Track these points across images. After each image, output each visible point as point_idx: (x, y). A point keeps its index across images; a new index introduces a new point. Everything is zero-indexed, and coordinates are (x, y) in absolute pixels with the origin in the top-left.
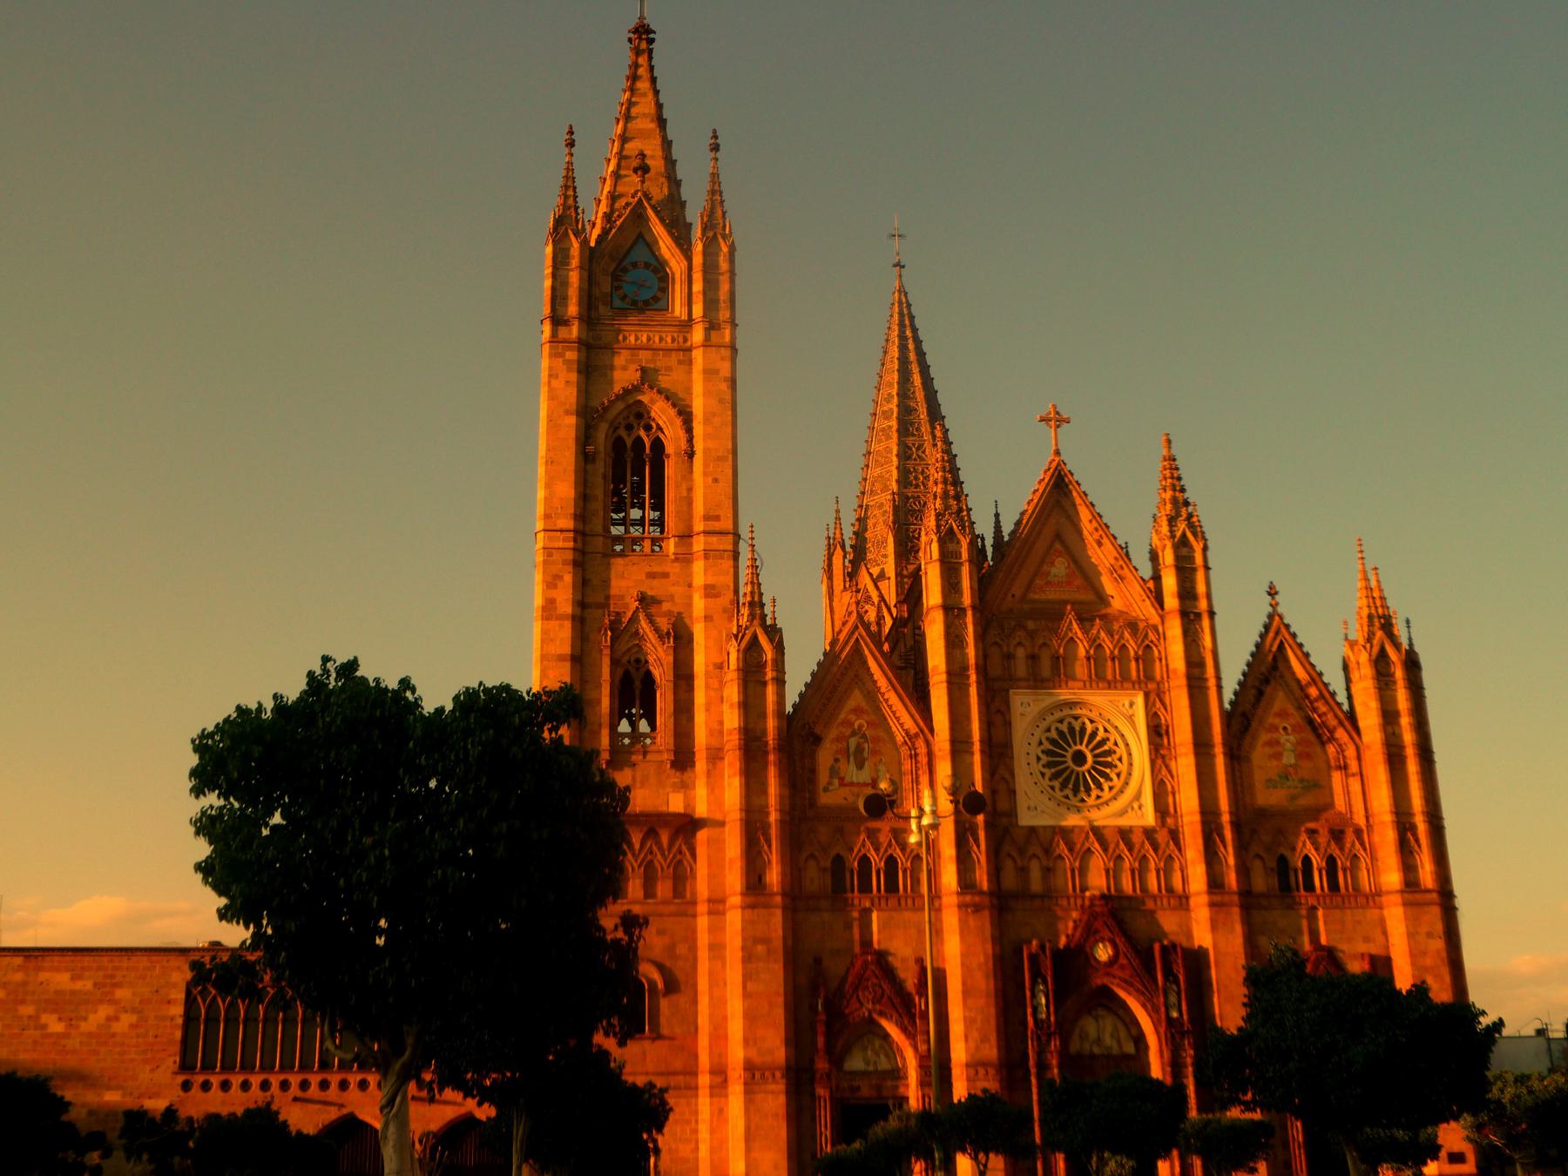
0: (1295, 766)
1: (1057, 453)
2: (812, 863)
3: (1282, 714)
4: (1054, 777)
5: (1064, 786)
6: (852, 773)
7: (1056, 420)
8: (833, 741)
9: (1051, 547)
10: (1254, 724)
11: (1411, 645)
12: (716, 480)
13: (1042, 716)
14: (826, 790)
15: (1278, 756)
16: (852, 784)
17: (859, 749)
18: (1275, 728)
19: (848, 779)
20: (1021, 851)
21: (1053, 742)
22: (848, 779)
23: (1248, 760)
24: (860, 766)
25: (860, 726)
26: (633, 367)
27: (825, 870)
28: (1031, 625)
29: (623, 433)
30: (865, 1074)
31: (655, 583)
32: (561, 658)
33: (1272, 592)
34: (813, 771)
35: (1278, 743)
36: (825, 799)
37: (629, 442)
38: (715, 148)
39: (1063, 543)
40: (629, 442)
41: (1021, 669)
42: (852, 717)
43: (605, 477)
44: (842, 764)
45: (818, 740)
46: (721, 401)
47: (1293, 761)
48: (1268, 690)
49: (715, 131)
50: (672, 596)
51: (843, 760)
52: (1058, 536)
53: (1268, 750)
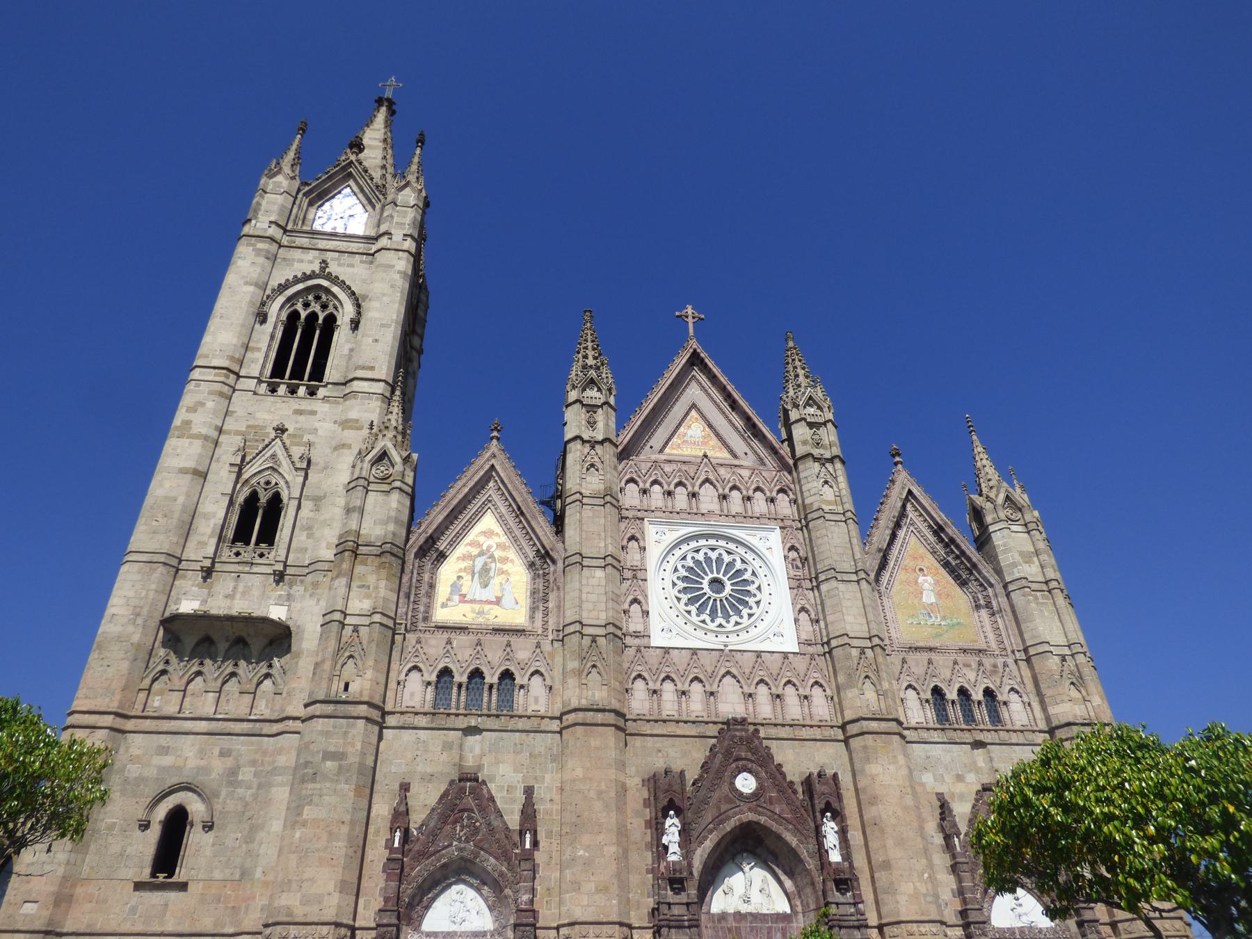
4: (691, 601)
5: (700, 611)
8: (458, 558)
9: (687, 414)
10: (891, 564)
13: (678, 545)
14: (444, 605)
16: (473, 601)
17: (485, 570)
19: (469, 597)
21: (690, 569)
22: (469, 597)
25: (489, 547)
27: (429, 683)
28: (668, 468)
29: (299, 307)
31: (302, 418)
32: (183, 471)
34: (432, 586)
36: (441, 615)
37: (303, 315)
39: (699, 411)
40: (303, 315)
42: (482, 539)
43: (272, 337)
44: (462, 581)
45: (442, 556)
46: (392, 286)
47: (933, 600)
48: (901, 534)
50: (316, 430)
51: (467, 577)
52: (694, 406)
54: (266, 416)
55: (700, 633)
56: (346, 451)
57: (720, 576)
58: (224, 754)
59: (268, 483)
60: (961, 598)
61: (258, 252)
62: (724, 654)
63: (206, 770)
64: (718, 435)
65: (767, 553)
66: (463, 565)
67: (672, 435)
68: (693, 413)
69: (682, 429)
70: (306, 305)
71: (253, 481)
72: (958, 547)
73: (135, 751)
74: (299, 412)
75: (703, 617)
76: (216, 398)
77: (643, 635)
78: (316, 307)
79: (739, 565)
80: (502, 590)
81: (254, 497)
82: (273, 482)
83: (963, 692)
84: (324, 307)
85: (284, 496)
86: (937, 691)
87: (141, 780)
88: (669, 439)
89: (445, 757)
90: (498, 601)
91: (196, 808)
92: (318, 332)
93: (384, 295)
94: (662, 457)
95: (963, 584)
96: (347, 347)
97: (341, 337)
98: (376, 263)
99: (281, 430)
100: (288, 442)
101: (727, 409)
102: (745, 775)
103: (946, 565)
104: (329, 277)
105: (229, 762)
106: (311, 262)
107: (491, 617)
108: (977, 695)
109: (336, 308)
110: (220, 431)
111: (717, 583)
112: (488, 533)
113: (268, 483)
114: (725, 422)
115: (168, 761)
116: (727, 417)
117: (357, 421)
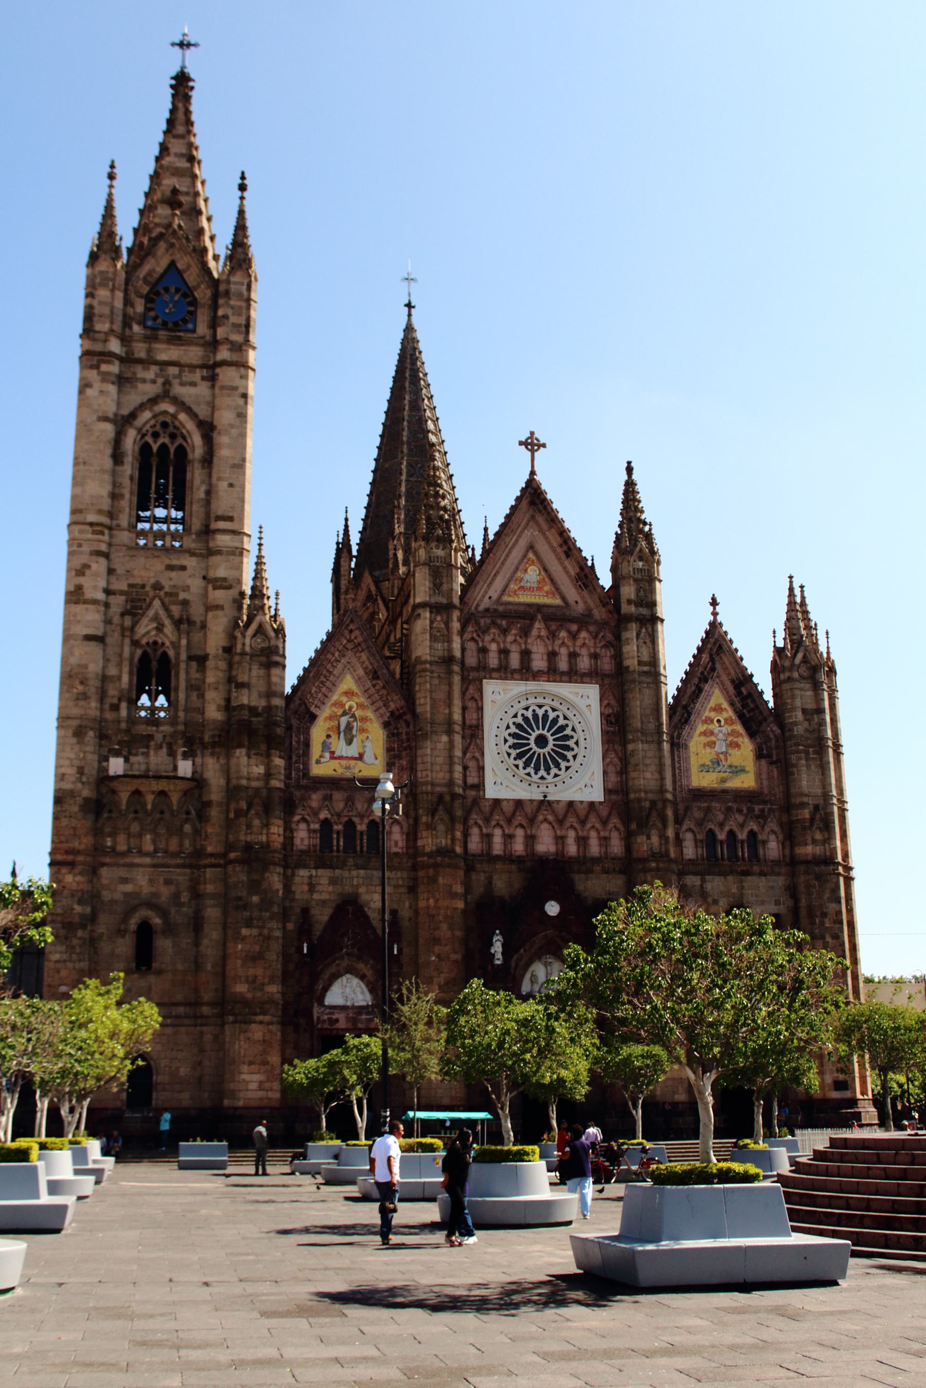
0: (725, 754)
1: (533, 473)
2: (303, 826)
3: (718, 709)
4: (519, 756)
6: (341, 748)
7: (532, 444)
8: (327, 719)
11: (828, 653)
12: (231, 485)
14: (318, 762)
15: (712, 744)
16: (340, 758)
17: (349, 727)
18: (709, 721)
19: (337, 754)
20: (487, 820)
22: (337, 754)
23: (686, 747)
24: (349, 742)
25: (351, 708)
26: (160, 381)
27: (315, 831)
29: (149, 439)
30: (343, 1008)
31: (173, 574)
32: (88, 638)
33: (714, 603)
34: (307, 745)
35: (712, 733)
36: (317, 770)
38: (242, 188)
39: (536, 553)
40: (155, 448)
41: (493, 660)
42: (344, 699)
43: (131, 478)
44: (331, 740)
45: (313, 718)
47: (724, 749)
48: (707, 687)
49: (243, 173)
50: (188, 587)
53: (703, 739)
54: (144, 574)
55: (525, 785)
56: (220, 613)
57: (545, 732)
58: (168, 882)
59: (155, 643)
60: (747, 748)
61: (105, 377)
62: (544, 804)
63: (156, 895)
64: (552, 580)
65: (586, 710)
66: (328, 724)
69: (519, 574)
70: (156, 435)
71: (144, 642)
72: (754, 701)
73: (105, 881)
74: (170, 568)
75: (528, 770)
76: (94, 558)
77: (480, 786)
78: (164, 439)
79: (561, 722)
80: (365, 747)
81: (145, 658)
82: (160, 641)
83: (731, 834)
84: (173, 437)
85: (171, 653)
86: (711, 833)
87: (113, 902)
88: (506, 586)
89: (331, 889)
90: (360, 757)
91: (157, 921)
92: (171, 469)
93: (232, 426)
95: (752, 734)
96: (203, 488)
97: (196, 475)
98: (218, 384)
99: (157, 586)
100: (166, 600)
101: (563, 556)
102: (553, 903)
103: (741, 717)
104: (176, 401)
105: (172, 888)
106: (154, 382)
107: (356, 771)
108: (742, 835)
109: (184, 438)
110: (108, 592)
111: (541, 741)
112: (349, 694)
113: (155, 643)
114: (560, 568)
115: (129, 888)
116: (562, 564)
117: (225, 579)
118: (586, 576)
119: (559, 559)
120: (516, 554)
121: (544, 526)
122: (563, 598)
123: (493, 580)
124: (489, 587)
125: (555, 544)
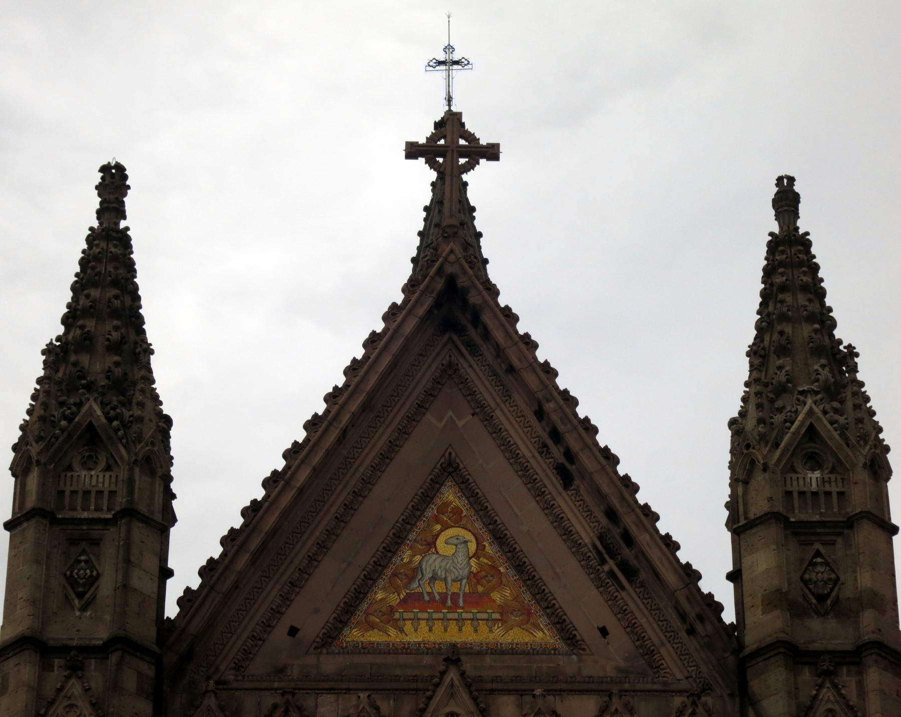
9: (427, 497)
52: (450, 469)
64: (520, 567)
67: (369, 580)
68: (450, 495)
88: (359, 594)
94: (329, 664)
101: (551, 482)
116: (548, 507)
118: (628, 539)
119: (539, 493)
120: (391, 494)
121: (488, 393)
122: (561, 625)
123: (305, 572)
124: (286, 599)
125: (527, 450)
